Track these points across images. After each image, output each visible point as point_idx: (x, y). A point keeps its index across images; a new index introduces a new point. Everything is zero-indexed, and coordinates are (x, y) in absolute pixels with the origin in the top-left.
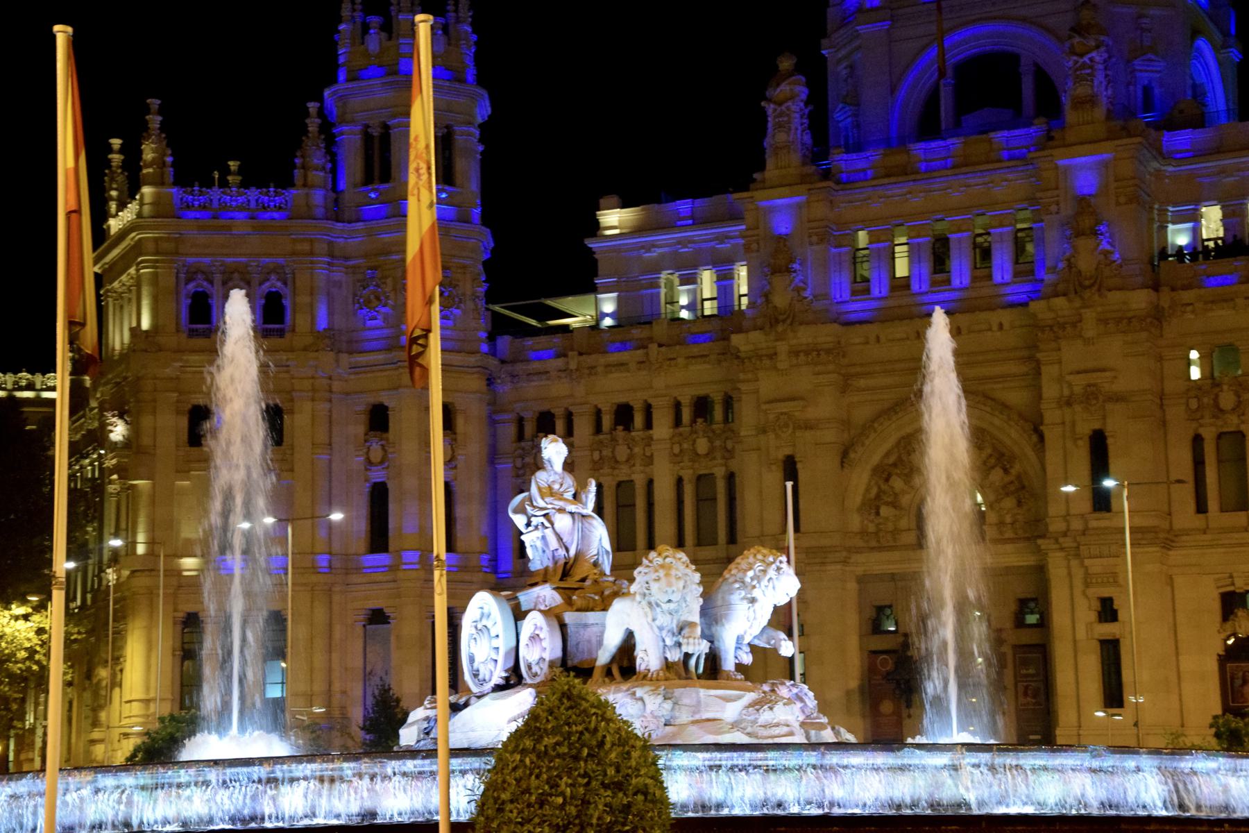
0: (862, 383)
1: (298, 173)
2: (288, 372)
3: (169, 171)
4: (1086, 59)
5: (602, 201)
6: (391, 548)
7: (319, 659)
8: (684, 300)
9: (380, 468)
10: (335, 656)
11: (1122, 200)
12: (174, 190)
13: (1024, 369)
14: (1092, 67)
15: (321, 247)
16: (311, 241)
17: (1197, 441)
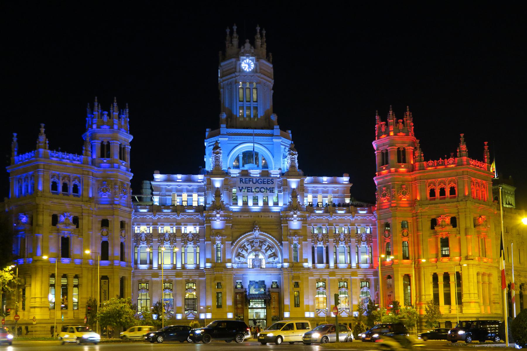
0: (236, 226)
1: (84, 152)
2: (81, 207)
3: (47, 145)
4: (293, 157)
5: (155, 172)
6: (109, 260)
7: (90, 289)
8: (178, 200)
9: (106, 237)
10: (93, 288)
11: (302, 190)
12: (49, 151)
13: (276, 227)
14: (295, 159)
15: (91, 173)
16: (88, 171)
17: (313, 248)
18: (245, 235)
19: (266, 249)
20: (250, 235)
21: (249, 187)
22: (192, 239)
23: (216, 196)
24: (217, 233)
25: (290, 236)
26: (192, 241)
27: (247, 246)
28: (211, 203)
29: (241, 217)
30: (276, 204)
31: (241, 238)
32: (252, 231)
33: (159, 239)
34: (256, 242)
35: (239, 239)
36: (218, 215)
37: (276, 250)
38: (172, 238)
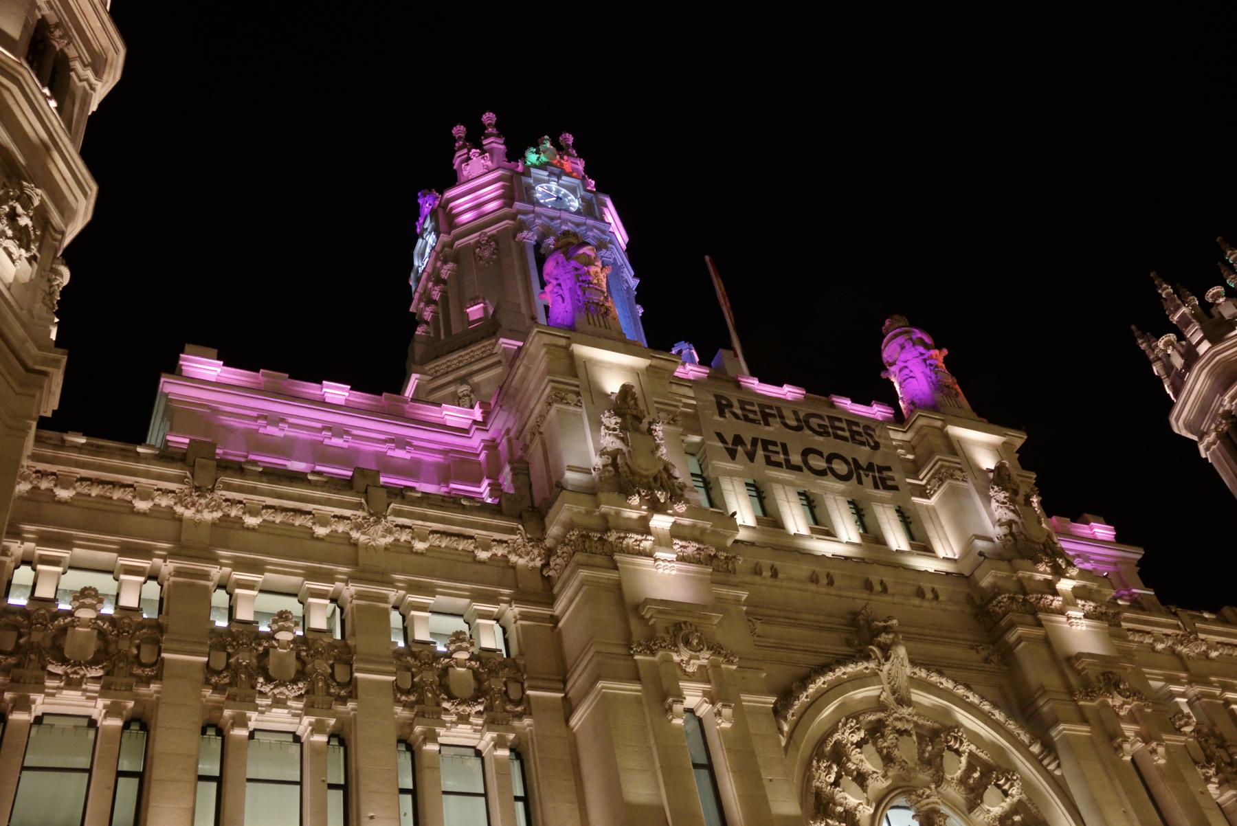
18: (830, 677)
19: (963, 781)
20: (859, 681)
21: (775, 444)
22: (473, 684)
23: (623, 428)
24: (678, 626)
25: (1089, 690)
26: (474, 700)
27: (856, 755)
28: (597, 461)
29: (775, 574)
30: (923, 547)
31: (812, 689)
32: (867, 658)
33: (220, 661)
34: (901, 733)
35: (804, 698)
36: (661, 523)
37: (1027, 786)
38: (323, 666)
